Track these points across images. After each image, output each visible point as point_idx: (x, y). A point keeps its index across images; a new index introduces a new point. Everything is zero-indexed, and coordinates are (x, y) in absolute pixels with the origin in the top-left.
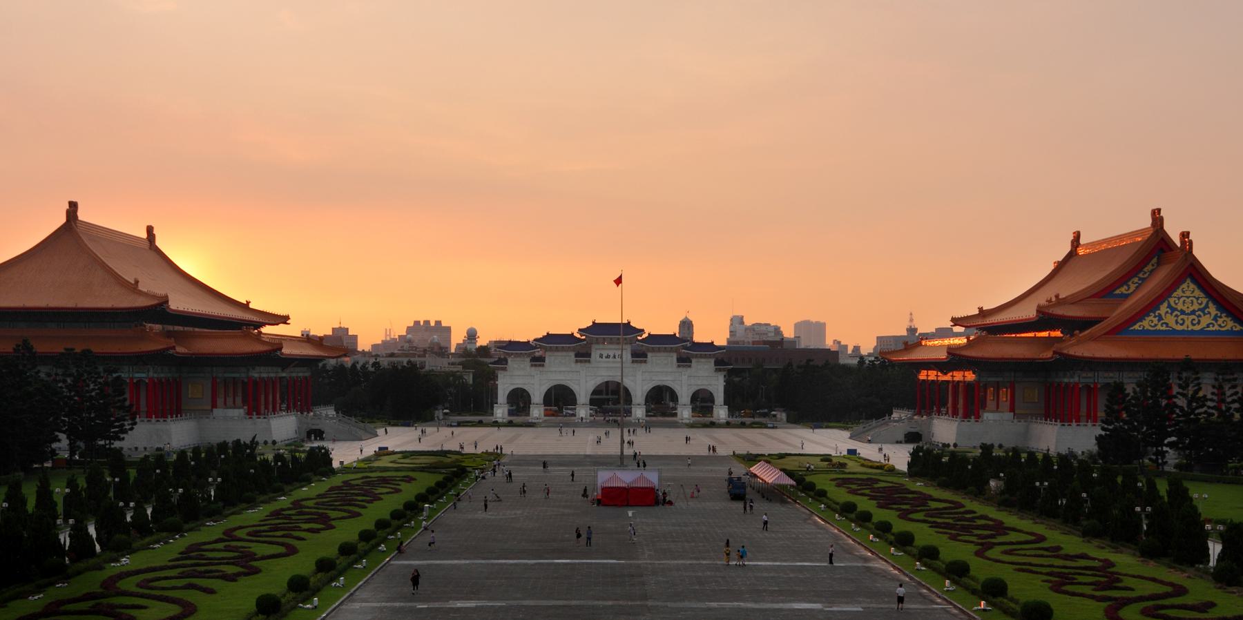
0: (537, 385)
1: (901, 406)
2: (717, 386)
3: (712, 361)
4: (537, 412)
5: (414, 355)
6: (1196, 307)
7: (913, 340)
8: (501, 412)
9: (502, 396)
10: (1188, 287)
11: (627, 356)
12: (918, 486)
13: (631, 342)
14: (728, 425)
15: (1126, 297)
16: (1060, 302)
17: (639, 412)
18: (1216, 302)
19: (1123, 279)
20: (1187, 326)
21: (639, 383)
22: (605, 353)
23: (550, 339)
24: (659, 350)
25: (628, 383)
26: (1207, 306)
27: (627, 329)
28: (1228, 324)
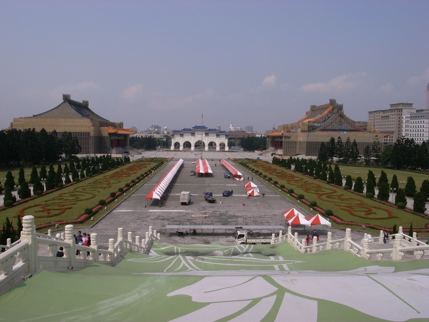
0: (181, 141)
2: (226, 142)
4: (181, 148)
8: (172, 148)
12: (275, 167)
14: (228, 151)
17: (207, 148)
21: (207, 141)
23: (185, 130)
24: (212, 133)
25: (204, 141)
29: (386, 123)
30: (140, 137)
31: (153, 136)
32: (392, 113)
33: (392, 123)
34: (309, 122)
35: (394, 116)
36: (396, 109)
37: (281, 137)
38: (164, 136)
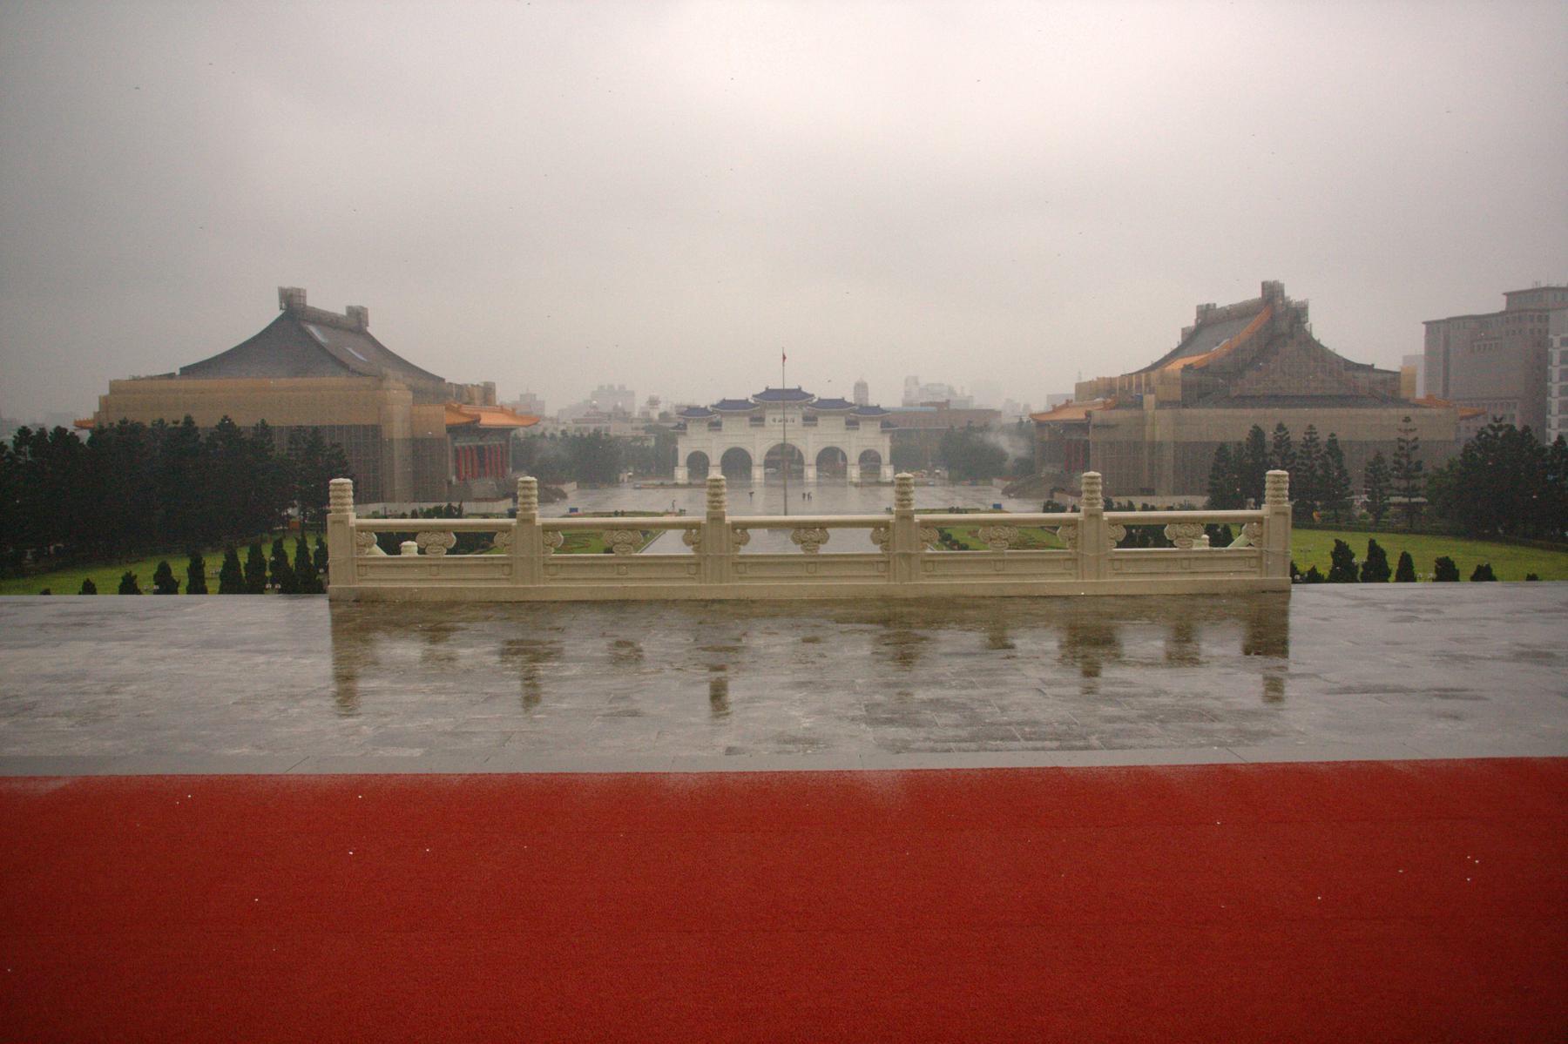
0: (715, 447)
5: (600, 421)
7: (995, 414)
8: (681, 474)
9: (682, 459)
11: (799, 419)
13: (801, 406)
17: (811, 473)
21: (810, 444)
22: (778, 417)
24: (830, 414)
25: (799, 444)
30: (559, 434)
31: (608, 429)
34: (1187, 368)
37: (1082, 426)
38: (648, 430)
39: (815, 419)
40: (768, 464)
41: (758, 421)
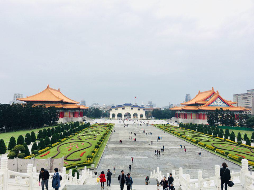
0: (116, 113)
1: (173, 117)
2: (144, 113)
3: (143, 110)
4: (116, 117)
6: (220, 102)
8: (111, 117)
10: (218, 99)
14: (146, 119)
15: (208, 100)
16: (198, 101)
18: (223, 101)
19: (208, 98)
20: (218, 105)
26: (221, 102)
27: (129, 105)
28: (225, 105)
29: (246, 102)
32: (249, 96)
33: (249, 102)
35: (250, 97)
36: (251, 93)
39: (133, 109)
40: (125, 116)
41: (123, 109)
